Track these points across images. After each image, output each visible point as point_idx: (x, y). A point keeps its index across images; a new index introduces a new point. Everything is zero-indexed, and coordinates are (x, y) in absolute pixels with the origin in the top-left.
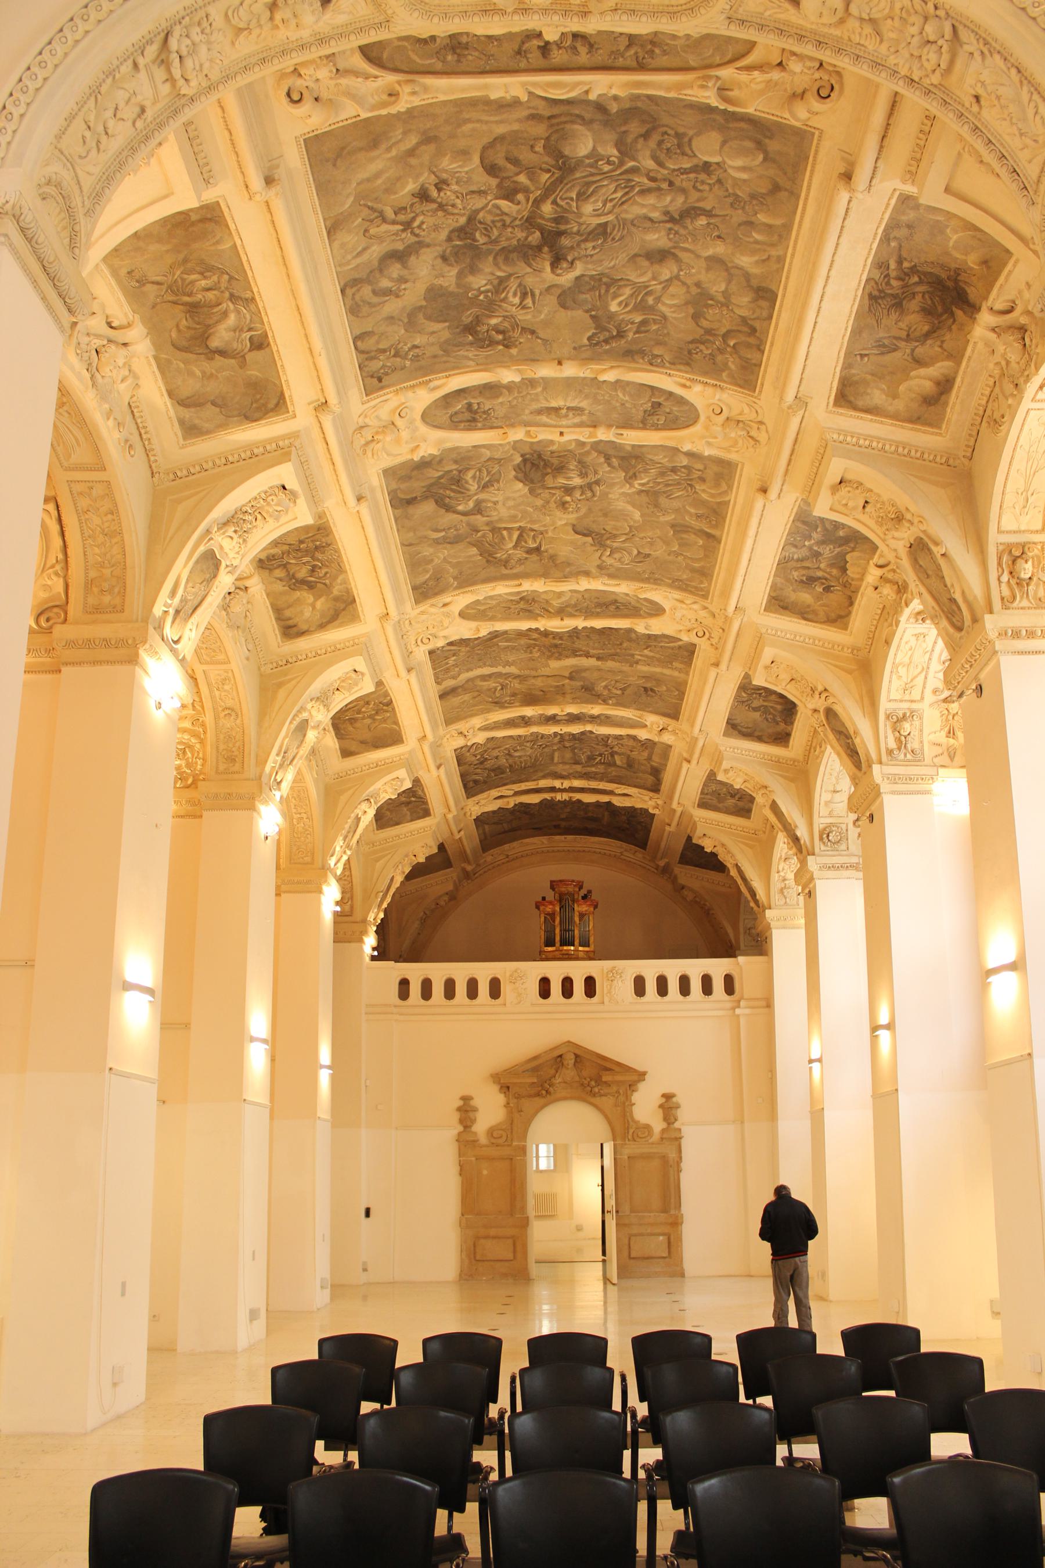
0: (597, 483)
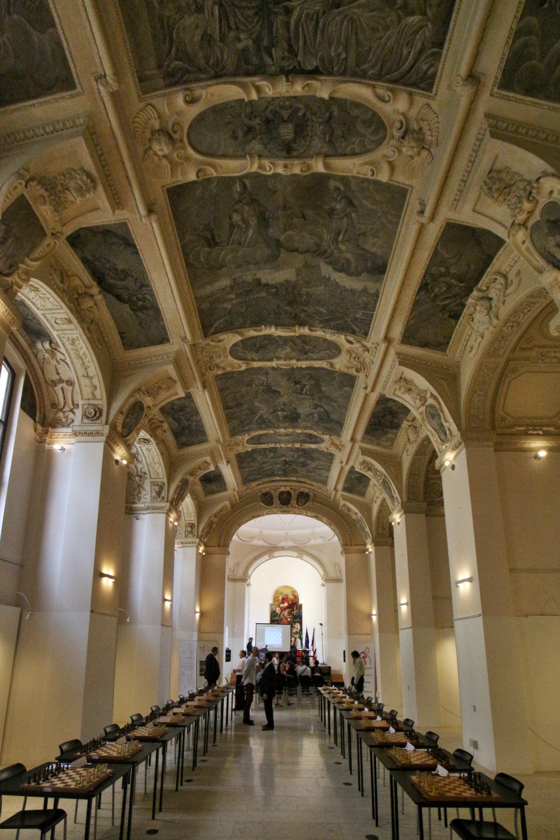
0: (272, 412)
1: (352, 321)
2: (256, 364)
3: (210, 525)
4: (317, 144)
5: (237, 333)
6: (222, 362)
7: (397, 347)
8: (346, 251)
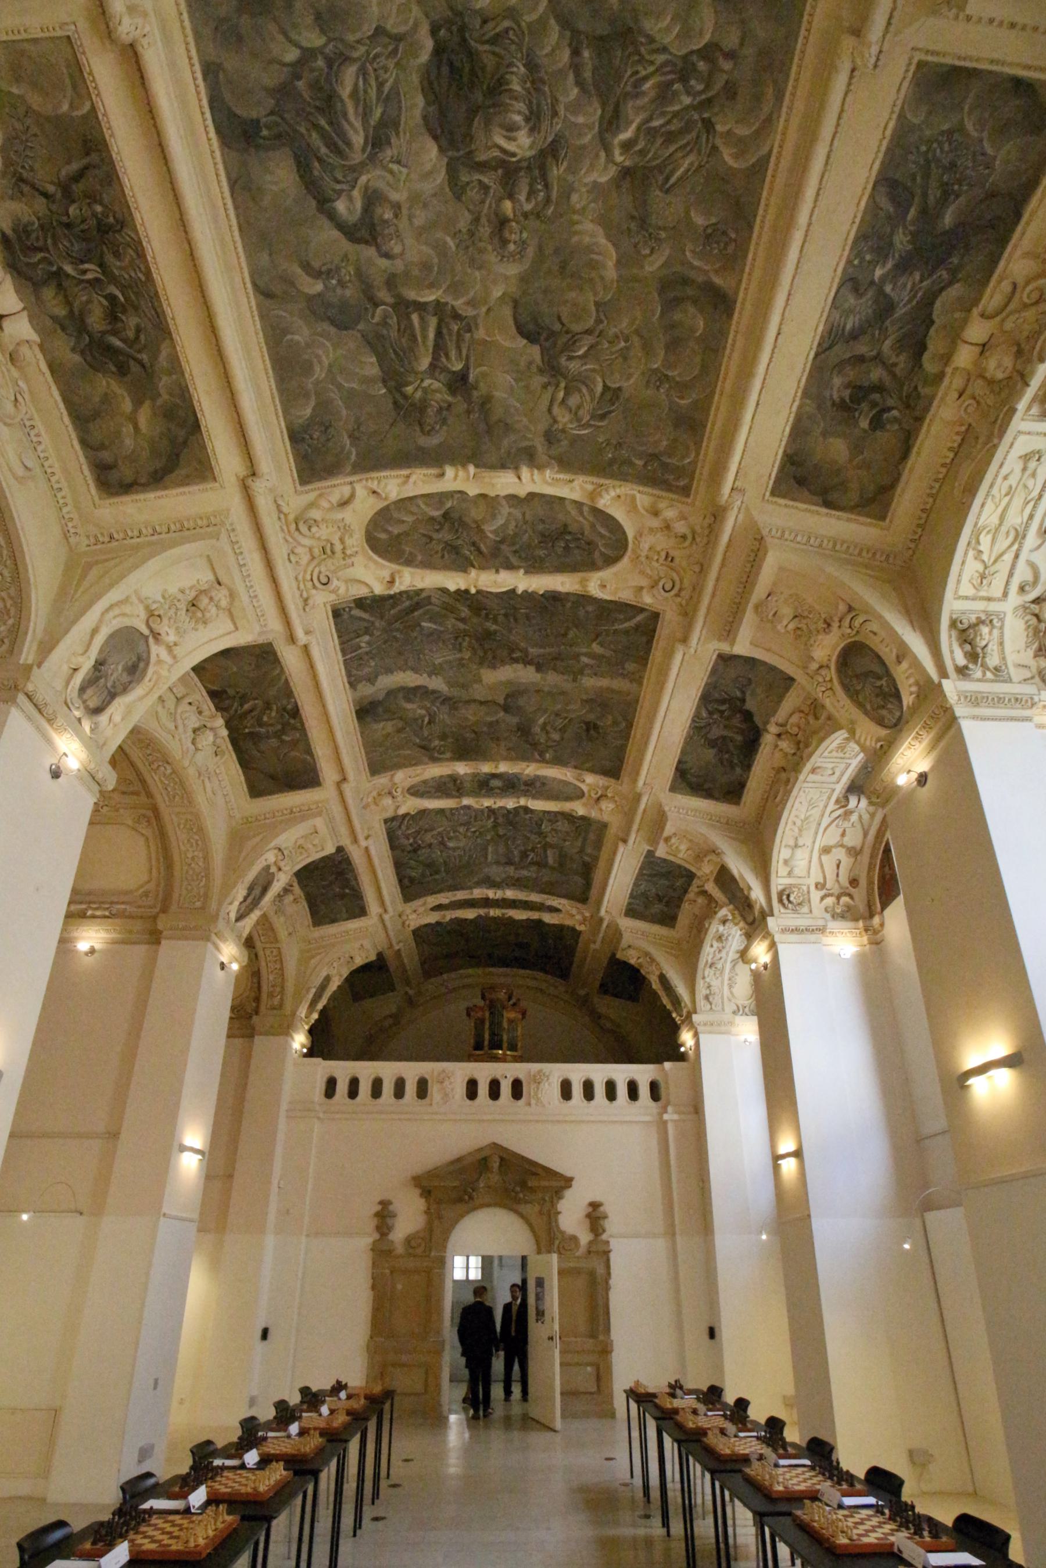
8: (414, 708)
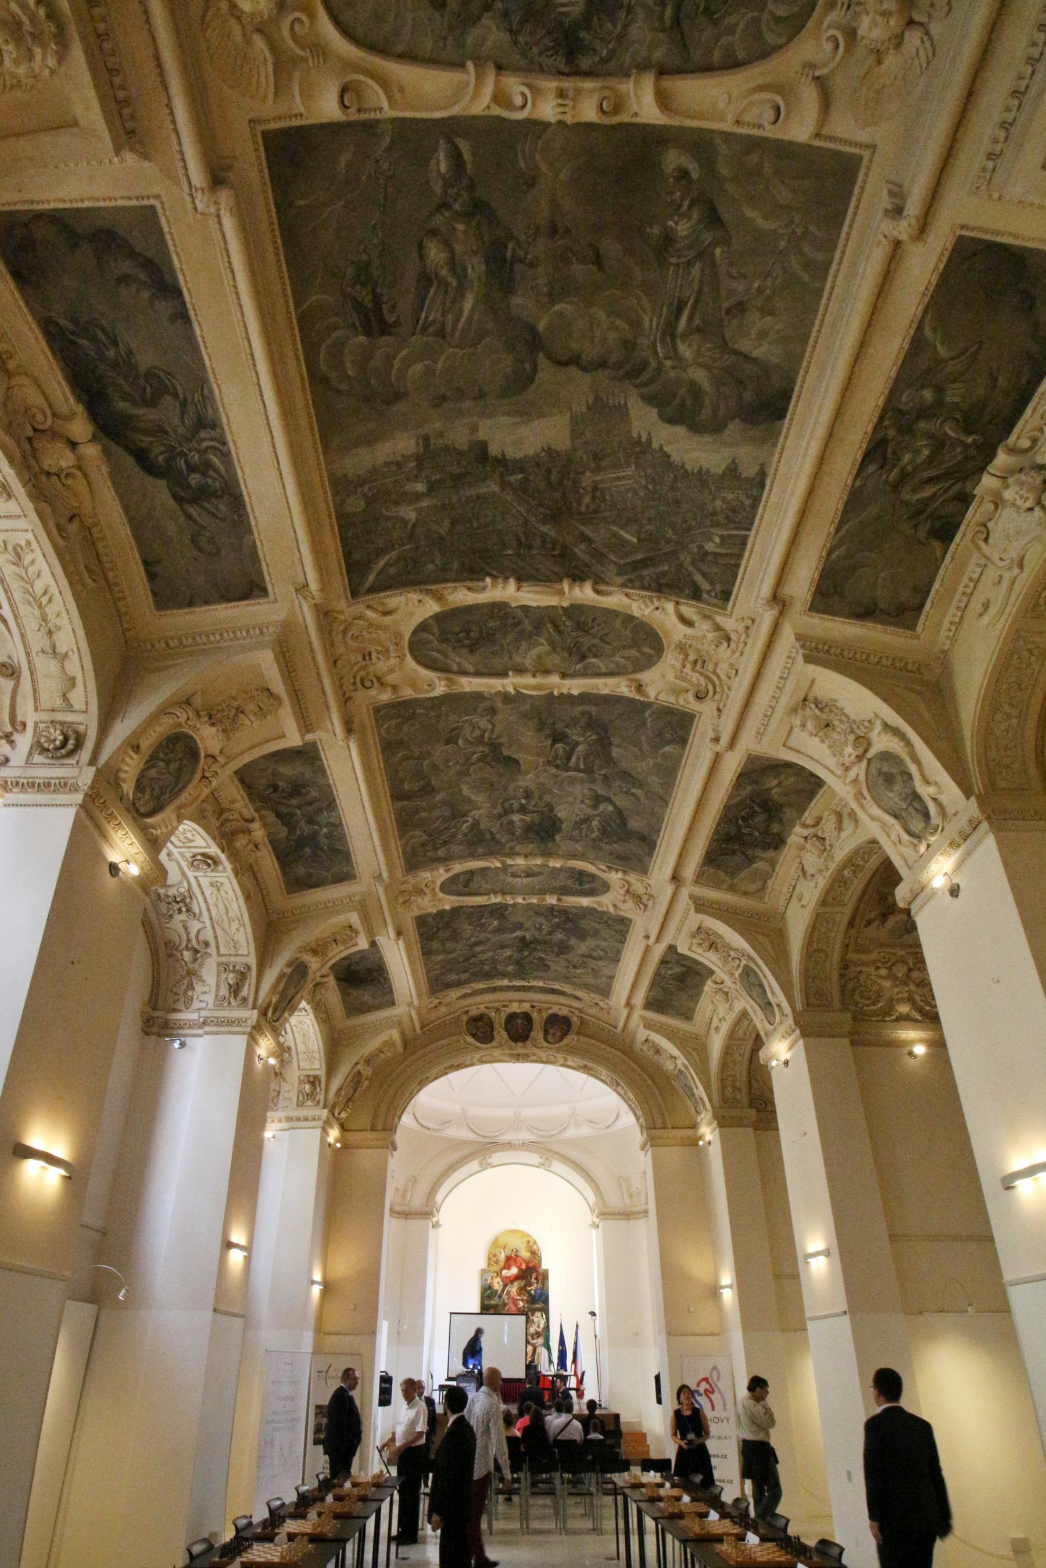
0: (500, 816)
1: (693, 563)
2: (469, 684)
3: (356, 1080)
4: (642, 33)
5: (428, 592)
6: (392, 671)
7: (801, 620)
